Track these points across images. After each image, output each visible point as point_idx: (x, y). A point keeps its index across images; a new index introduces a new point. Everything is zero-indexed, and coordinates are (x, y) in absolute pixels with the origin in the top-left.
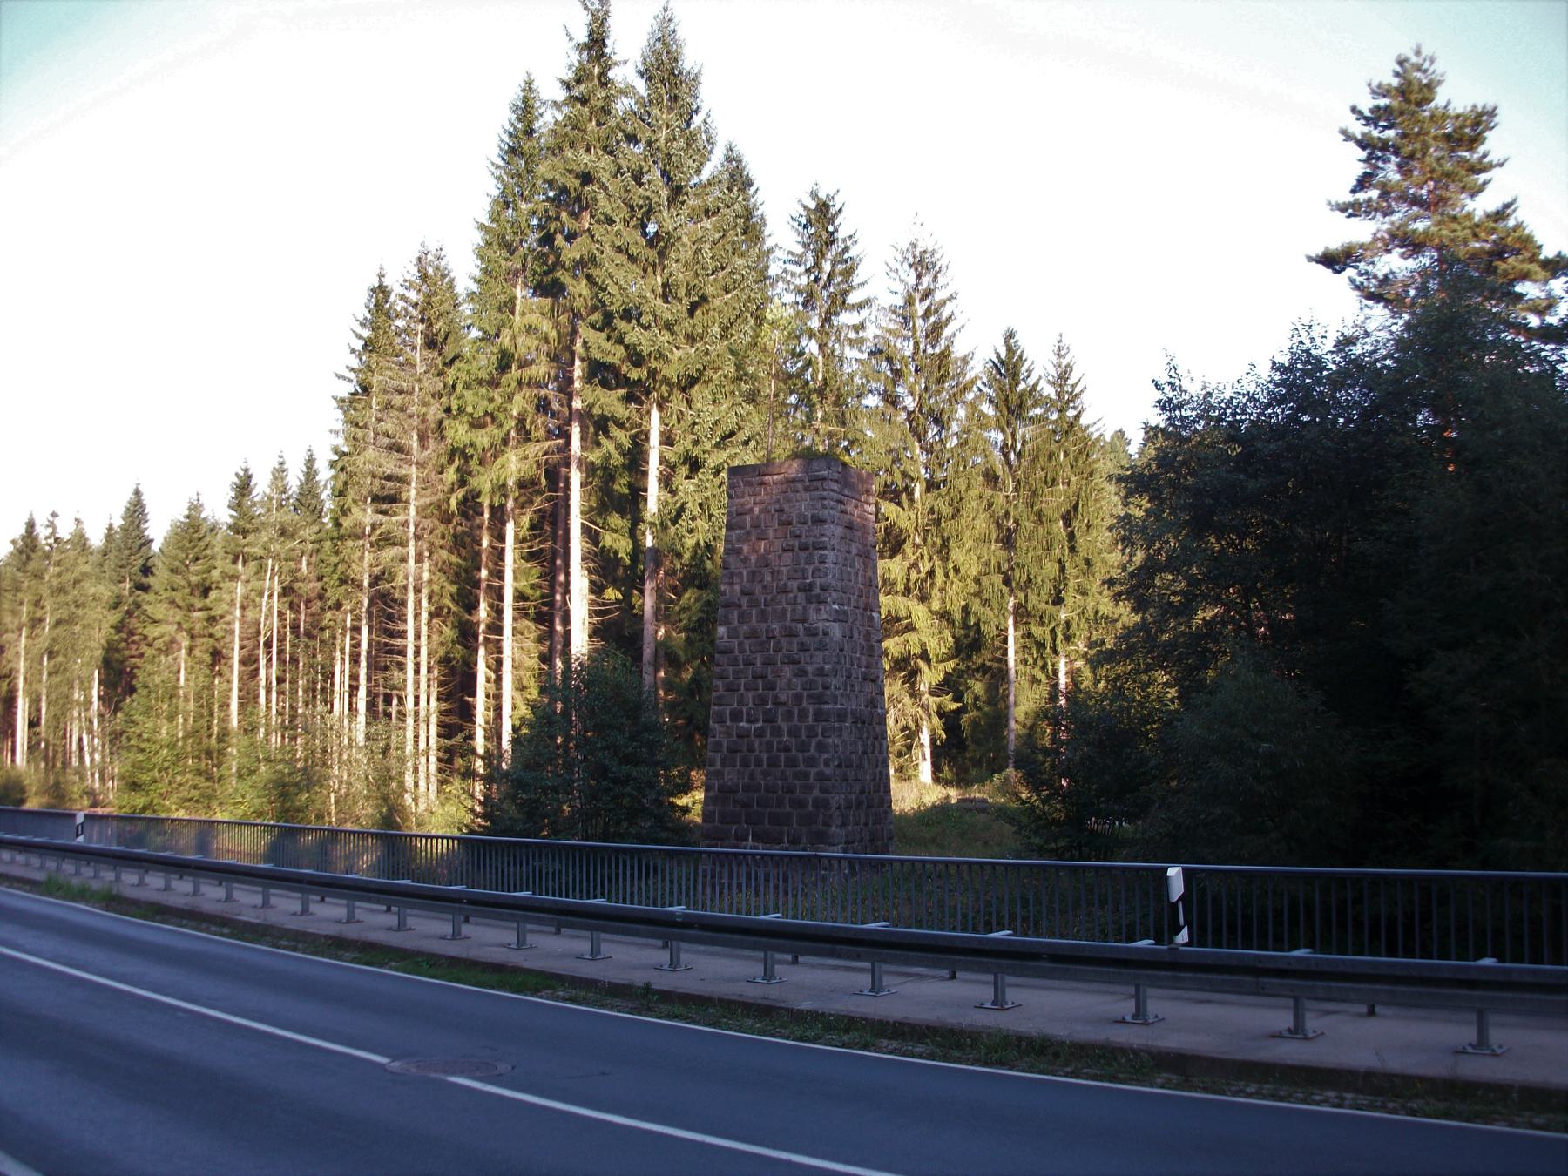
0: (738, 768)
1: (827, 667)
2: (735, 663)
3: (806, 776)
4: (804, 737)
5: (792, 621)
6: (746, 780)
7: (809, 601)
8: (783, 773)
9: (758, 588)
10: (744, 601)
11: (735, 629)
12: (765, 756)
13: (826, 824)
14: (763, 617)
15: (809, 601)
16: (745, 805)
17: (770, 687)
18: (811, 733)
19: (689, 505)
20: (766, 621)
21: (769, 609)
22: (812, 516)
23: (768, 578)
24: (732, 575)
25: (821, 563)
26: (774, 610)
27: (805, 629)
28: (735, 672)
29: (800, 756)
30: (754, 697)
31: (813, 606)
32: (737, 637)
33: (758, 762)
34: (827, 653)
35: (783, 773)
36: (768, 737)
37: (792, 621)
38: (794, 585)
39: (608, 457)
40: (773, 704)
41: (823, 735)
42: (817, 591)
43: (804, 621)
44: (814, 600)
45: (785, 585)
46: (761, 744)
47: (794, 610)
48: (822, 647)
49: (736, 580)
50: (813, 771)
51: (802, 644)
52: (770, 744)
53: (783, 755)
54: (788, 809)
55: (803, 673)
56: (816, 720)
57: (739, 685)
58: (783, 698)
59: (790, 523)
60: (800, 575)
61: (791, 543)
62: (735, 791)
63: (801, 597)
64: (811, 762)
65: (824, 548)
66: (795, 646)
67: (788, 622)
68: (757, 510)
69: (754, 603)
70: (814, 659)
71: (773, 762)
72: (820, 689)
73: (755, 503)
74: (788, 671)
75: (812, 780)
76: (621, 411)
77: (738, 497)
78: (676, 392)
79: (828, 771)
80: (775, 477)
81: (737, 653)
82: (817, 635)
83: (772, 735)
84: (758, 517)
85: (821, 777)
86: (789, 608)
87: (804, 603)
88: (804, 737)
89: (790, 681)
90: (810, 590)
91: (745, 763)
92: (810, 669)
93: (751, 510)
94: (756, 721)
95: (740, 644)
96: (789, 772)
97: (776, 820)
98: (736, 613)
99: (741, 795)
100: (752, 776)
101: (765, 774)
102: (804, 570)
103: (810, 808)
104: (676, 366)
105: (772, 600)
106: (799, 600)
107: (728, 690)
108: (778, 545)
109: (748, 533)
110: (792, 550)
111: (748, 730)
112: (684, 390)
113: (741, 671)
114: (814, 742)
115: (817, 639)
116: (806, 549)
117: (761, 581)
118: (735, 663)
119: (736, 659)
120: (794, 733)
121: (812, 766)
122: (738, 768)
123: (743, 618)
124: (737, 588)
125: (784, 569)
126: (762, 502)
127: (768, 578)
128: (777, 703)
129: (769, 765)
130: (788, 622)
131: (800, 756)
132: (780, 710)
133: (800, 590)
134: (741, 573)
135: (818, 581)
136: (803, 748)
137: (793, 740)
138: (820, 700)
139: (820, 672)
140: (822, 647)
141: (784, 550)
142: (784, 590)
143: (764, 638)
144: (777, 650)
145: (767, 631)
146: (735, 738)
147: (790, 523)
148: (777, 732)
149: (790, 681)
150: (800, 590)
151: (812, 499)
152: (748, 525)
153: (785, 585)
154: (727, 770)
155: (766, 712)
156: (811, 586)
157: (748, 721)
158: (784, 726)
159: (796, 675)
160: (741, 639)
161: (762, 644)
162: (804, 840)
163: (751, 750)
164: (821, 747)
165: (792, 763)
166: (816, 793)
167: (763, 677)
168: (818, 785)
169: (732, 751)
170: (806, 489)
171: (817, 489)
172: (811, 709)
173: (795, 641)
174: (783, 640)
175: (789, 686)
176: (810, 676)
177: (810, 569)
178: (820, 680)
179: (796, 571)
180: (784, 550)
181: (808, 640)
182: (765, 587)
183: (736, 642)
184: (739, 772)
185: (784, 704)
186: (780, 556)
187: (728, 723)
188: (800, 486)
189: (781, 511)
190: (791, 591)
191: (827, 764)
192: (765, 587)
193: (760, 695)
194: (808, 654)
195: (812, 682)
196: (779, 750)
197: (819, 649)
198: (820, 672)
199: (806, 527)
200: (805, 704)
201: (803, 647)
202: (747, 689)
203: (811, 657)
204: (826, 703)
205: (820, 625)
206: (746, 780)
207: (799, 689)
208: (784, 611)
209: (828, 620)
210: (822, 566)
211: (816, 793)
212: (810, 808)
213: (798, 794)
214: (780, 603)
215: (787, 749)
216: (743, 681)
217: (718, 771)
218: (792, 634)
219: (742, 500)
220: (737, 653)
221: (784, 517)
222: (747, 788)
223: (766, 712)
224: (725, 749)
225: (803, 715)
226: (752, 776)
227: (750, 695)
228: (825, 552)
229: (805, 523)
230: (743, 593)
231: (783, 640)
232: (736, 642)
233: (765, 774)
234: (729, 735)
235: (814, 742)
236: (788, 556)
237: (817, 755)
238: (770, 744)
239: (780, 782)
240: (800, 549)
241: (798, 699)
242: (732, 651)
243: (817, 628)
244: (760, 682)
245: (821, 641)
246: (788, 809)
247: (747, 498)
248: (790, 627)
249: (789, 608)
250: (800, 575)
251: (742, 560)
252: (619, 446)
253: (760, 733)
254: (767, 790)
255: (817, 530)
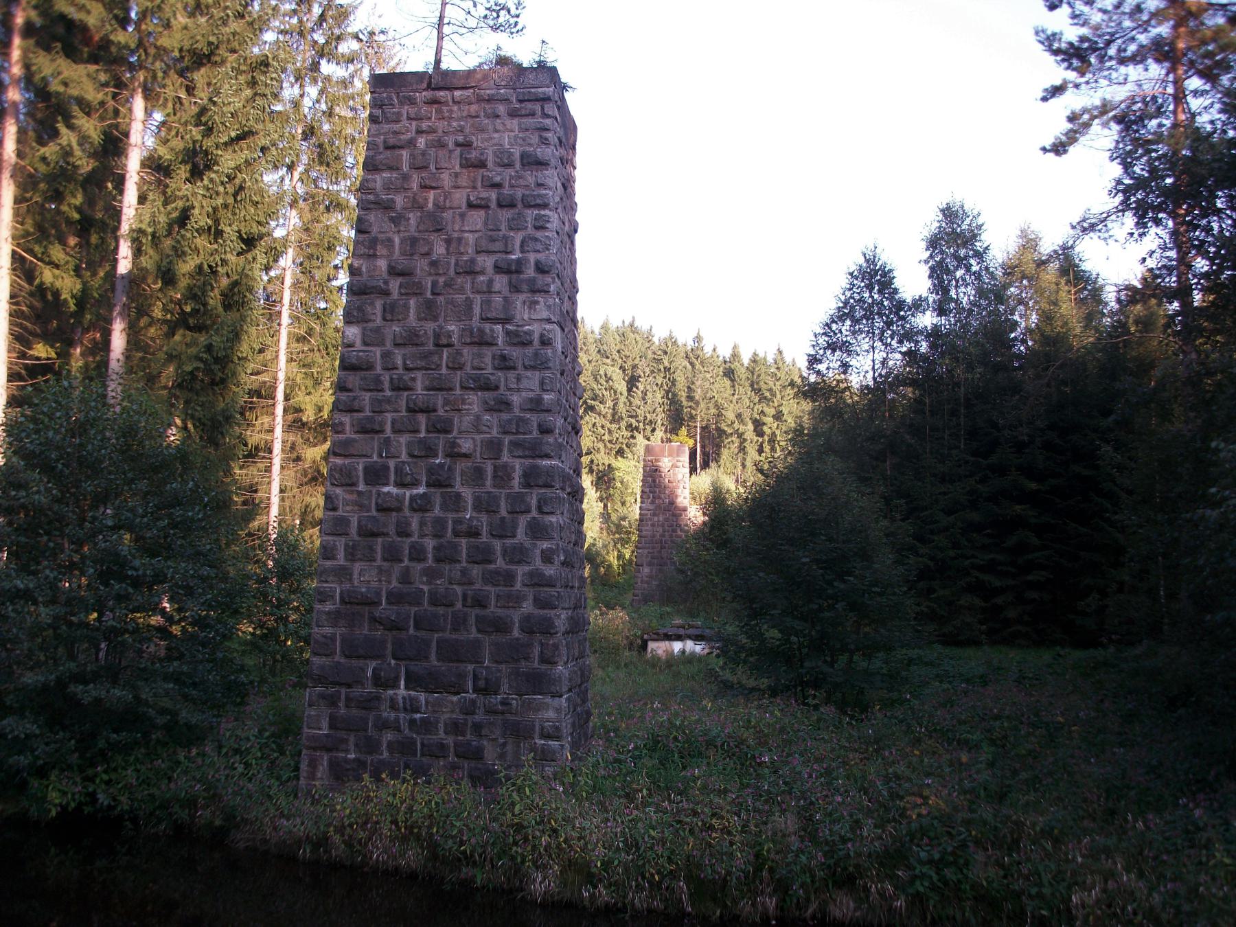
0: (379, 562)
1: (547, 397)
2: (376, 386)
3: (509, 578)
4: (504, 513)
5: (484, 319)
6: (394, 584)
7: (515, 289)
8: (464, 572)
9: (421, 265)
10: (395, 285)
11: (377, 330)
12: (430, 543)
13: (547, 660)
14: (429, 310)
15: (515, 289)
16: (395, 626)
17: (442, 428)
18: (518, 506)
19: (196, 212)
20: (435, 319)
21: (441, 299)
22: (522, 156)
23: (440, 250)
24: (374, 242)
25: (537, 228)
26: (452, 302)
27: (508, 333)
28: (374, 402)
29: (497, 545)
30: (409, 445)
31: (522, 297)
32: (381, 343)
33: (417, 554)
34: (548, 374)
35: (464, 572)
36: (437, 511)
37: (484, 319)
38: (487, 262)
39: (67, 153)
40: (447, 455)
41: (540, 510)
42: (530, 272)
43: (505, 321)
44: (525, 287)
45: (473, 261)
46: (422, 524)
47: (487, 303)
48: (539, 364)
49: (381, 250)
50: (521, 570)
51: (504, 358)
52: (440, 523)
53: (464, 542)
54: (474, 634)
55: (504, 405)
56: (527, 485)
57: (382, 424)
58: (466, 445)
59: (482, 164)
60: (498, 246)
61: (484, 195)
62: (375, 603)
63: (500, 282)
64: (518, 555)
65: (545, 206)
66: (488, 360)
67: (475, 322)
68: (421, 142)
69: (413, 289)
70: (525, 383)
71: (446, 555)
72: (535, 433)
73: (420, 132)
74: (474, 402)
75: (518, 586)
76: (93, 95)
77: (389, 121)
78: (173, 75)
79: (550, 571)
80: (457, 93)
81: (379, 370)
82: (530, 343)
83: (444, 507)
84: (423, 154)
85: (537, 580)
86: (478, 299)
87: (505, 292)
88: (504, 513)
89: (478, 418)
90: (518, 272)
91: (392, 555)
92: (516, 399)
93: (411, 143)
94: (415, 484)
95: (386, 355)
96: (476, 571)
97: (452, 653)
98: (379, 304)
99: (384, 609)
100: (405, 578)
101: (431, 574)
102: (506, 239)
103: (516, 633)
104: (178, 36)
105: (448, 285)
106: (497, 286)
107: (364, 431)
108: (460, 198)
109: (406, 177)
110: (486, 207)
111: (399, 499)
112: (181, 74)
113: (388, 401)
114: (523, 521)
115: (530, 351)
116: (512, 205)
117: (427, 254)
118: (376, 386)
119: (378, 380)
120: (485, 505)
121: (519, 562)
122: (379, 562)
123: (391, 312)
124: (382, 264)
125: (471, 237)
126: (432, 131)
127: (440, 250)
128: (454, 454)
129: (438, 560)
130: (475, 322)
131: (497, 545)
132: (461, 465)
133: (498, 269)
134: (390, 240)
135: (532, 257)
136: (503, 531)
137: (484, 518)
138: (535, 451)
139: (536, 405)
140: (539, 364)
141: (471, 206)
142: (470, 271)
143: (430, 346)
144: (456, 367)
145: (437, 336)
146: (374, 513)
147: (482, 164)
148: (455, 502)
149: (478, 418)
150: (498, 269)
151: (521, 130)
152: (405, 168)
153: (473, 261)
154: (357, 567)
155: (431, 471)
156: (520, 264)
157: (400, 484)
158: (467, 494)
159: (490, 410)
160: (389, 346)
161: (426, 356)
162: (505, 687)
163: (403, 532)
164: (538, 531)
165: (482, 556)
166: (527, 607)
167: (428, 410)
168: (530, 593)
169: (368, 533)
170: (513, 114)
171: (532, 114)
172: (518, 466)
173: (488, 353)
174: (466, 351)
175: (477, 427)
176: (517, 411)
177: (518, 238)
178: (534, 419)
179: (492, 240)
180: (471, 206)
181: (515, 353)
182: (434, 264)
183: (378, 351)
184: (380, 570)
185: (465, 456)
186: (462, 216)
187: (362, 487)
188: (501, 109)
189: (467, 145)
190: (482, 272)
191: (547, 558)
192: (434, 264)
193: (421, 441)
194: (511, 375)
195: (520, 421)
196: (456, 534)
197: (533, 368)
198: (536, 405)
199: (511, 172)
200: (505, 457)
201: (504, 363)
202: (397, 431)
203: (519, 379)
204: (548, 456)
205: (535, 328)
206: (394, 584)
207: (495, 432)
208: (469, 304)
209: (549, 321)
210: (539, 234)
211: (527, 607)
212: (516, 633)
213: (493, 609)
214: (461, 290)
215: (474, 533)
216: (389, 417)
217: (343, 568)
218: (483, 341)
219: (396, 127)
220: (379, 370)
221: (473, 155)
222: (396, 598)
223: (431, 471)
224: (353, 530)
225: (502, 475)
226: (405, 578)
227: (404, 439)
228: (546, 212)
229: (510, 165)
230: (393, 271)
231: (466, 351)
232: (378, 351)
233: (431, 574)
234: (362, 507)
235: (523, 521)
236: (477, 218)
237: (528, 544)
238: (440, 523)
239: (459, 590)
240: (500, 205)
241: (493, 448)
242: (370, 367)
243: (529, 333)
244: (422, 419)
245: (536, 354)
246: (474, 634)
247: (405, 122)
248: (481, 331)
249: (478, 299)
250: (498, 246)
251: (392, 220)
252: (83, 139)
253: (421, 505)
254: (434, 601)
255: (530, 178)
